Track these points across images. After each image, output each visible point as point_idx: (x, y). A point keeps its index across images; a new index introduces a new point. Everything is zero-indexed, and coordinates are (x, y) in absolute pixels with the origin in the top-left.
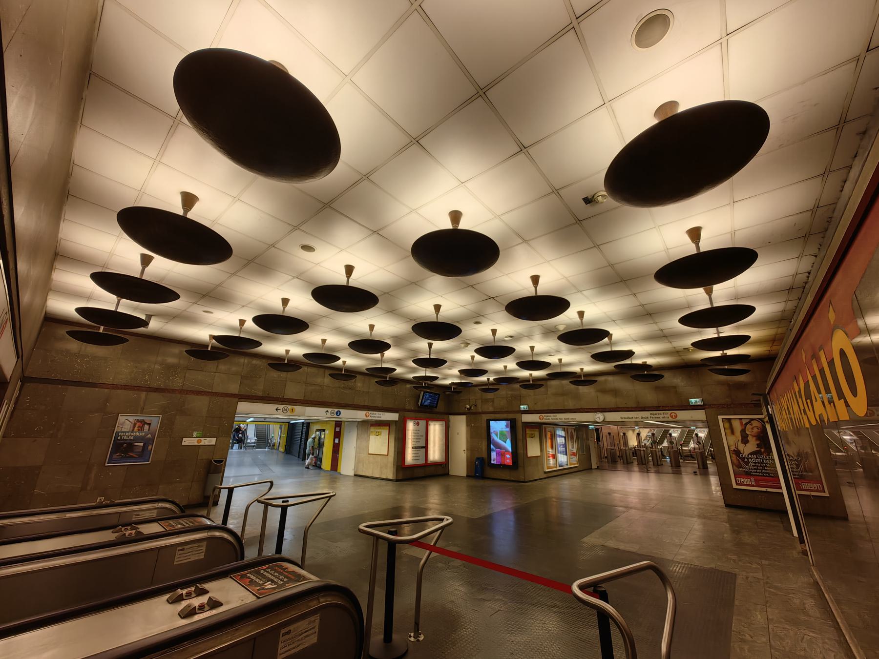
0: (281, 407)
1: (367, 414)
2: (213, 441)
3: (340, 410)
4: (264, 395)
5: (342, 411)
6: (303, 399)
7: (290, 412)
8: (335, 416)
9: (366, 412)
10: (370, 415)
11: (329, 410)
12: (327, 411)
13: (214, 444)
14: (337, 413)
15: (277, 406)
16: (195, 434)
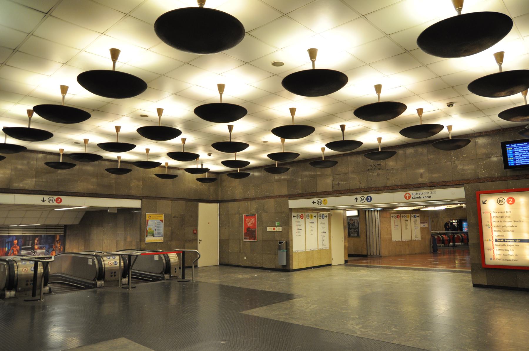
0: (316, 200)
1: (407, 195)
2: (279, 229)
3: (372, 195)
5: (372, 196)
6: (331, 190)
7: (324, 204)
8: (366, 202)
9: (405, 193)
10: (412, 196)
11: (359, 197)
12: (356, 198)
13: (281, 231)
14: (367, 199)
15: (312, 200)
16: (277, 224)
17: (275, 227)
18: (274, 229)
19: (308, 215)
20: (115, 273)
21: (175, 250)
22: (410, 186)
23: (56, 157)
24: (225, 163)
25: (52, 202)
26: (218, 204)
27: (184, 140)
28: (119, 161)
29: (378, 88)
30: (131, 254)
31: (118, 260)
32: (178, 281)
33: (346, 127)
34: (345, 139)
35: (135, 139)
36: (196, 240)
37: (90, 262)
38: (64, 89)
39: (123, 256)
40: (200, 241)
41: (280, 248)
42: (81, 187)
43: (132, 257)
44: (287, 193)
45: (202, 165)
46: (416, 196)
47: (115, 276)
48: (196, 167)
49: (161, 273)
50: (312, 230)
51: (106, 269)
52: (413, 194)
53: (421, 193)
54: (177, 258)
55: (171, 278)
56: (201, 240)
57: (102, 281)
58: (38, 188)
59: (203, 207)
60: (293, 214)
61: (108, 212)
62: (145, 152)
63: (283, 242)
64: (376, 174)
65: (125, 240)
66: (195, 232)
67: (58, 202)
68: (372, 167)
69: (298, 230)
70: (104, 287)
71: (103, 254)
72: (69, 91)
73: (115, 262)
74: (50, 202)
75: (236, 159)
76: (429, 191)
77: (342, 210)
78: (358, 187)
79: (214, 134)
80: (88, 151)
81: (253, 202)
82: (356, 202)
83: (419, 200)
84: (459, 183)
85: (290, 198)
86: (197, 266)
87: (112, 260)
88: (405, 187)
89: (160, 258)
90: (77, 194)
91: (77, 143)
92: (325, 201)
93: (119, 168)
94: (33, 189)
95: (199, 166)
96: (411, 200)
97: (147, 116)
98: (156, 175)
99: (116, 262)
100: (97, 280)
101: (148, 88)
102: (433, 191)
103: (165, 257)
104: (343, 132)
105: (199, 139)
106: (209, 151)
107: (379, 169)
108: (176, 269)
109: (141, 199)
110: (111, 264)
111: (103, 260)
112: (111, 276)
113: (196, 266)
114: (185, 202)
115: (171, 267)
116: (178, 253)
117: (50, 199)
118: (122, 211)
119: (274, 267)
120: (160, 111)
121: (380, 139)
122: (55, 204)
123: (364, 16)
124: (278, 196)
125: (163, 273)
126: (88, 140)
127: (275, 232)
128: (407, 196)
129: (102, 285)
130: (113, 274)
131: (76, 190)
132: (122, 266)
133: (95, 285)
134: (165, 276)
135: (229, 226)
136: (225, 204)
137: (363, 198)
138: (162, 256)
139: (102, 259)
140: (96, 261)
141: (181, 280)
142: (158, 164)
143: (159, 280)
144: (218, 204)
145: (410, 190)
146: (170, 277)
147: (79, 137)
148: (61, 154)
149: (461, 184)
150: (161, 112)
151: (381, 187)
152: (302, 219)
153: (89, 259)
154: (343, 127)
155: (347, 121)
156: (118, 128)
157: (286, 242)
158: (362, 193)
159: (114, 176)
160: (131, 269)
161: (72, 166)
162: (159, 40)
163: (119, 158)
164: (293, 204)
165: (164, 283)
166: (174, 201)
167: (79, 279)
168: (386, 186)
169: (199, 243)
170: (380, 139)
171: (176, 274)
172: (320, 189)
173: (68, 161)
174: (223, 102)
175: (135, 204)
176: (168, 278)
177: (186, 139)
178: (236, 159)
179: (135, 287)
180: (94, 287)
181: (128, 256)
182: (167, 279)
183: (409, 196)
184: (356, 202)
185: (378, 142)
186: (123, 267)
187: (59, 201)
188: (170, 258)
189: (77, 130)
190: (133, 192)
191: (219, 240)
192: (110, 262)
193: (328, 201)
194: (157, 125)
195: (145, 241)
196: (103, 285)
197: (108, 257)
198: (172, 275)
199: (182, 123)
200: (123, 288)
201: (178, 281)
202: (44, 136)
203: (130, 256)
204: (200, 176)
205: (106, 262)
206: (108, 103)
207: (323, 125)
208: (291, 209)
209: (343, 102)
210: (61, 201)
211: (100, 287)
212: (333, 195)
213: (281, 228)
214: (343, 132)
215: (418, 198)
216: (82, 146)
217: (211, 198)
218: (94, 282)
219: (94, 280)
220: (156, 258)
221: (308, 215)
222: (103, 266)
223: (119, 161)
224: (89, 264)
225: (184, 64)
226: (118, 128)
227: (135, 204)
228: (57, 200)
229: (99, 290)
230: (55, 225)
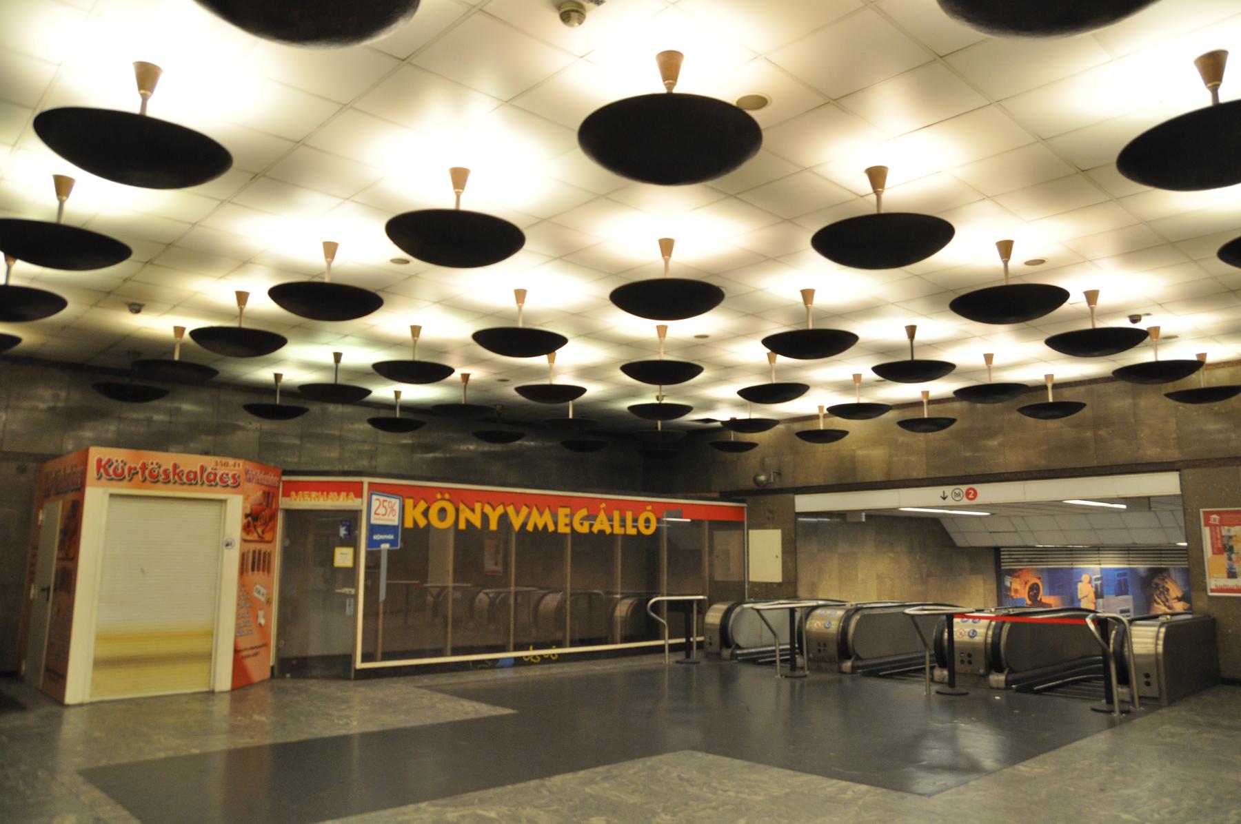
42: (1012, 460)
58: (933, 474)
67: (971, 496)
75: (1093, 324)
90: (1006, 475)
94: (925, 476)
117: (955, 493)
129: (943, 679)
178: (1093, 324)
187: (971, 495)
192: (961, 631)
195: (1205, 589)
202: (794, 390)
227: (1166, 484)
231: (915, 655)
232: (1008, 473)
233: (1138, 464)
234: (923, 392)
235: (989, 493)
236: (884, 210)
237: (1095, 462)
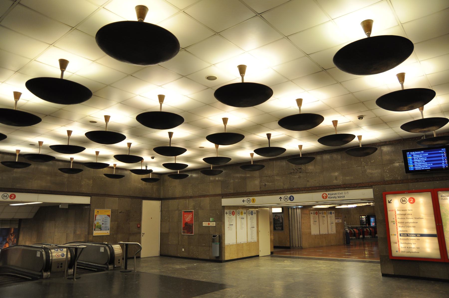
0: (245, 199)
1: (325, 195)
2: (213, 224)
3: (293, 195)
4: (234, 192)
5: (294, 195)
6: (259, 190)
8: (289, 201)
9: (323, 193)
10: (328, 196)
11: (282, 196)
12: (281, 198)
14: (290, 198)
15: (242, 199)
16: (211, 219)
17: (210, 223)
18: (209, 224)
19: (239, 212)
20: (62, 264)
21: (119, 243)
22: (327, 187)
23: (13, 157)
24: (166, 165)
25: (6, 198)
26: (161, 201)
27: (129, 144)
28: (72, 162)
29: (299, 102)
30: (77, 247)
31: (65, 252)
32: (121, 272)
33: (272, 136)
34: (271, 146)
35: (86, 142)
36: (140, 233)
37: (38, 255)
38: (17, 95)
39: (70, 248)
40: (143, 234)
41: (213, 241)
42: (35, 184)
43: (78, 249)
44: (220, 193)
45: (146, 167)
46: (332, 196)
47: (61, 267)
48: (141, 169)
49: (106, 264)
50: (242, 225)
51: (53, 261)
52: (330, 194)
53: (336, 193)
54: (120, 250)
55: (115, 269)
56: (144, 234)
57: (49, 272)
59: (146, 204)
60: (226, 211)
61: (60, 207)
62: (95, 154)
63: (217, 236)
64: (298, 176)
65: (75, 233)
66: (139, 226)
67: (12, 198)
68: (294, 171)
69: (230, 225)
70: (50, 278)
71: (52, 246)
72: (22, 97)
73: (62, 254)
74: (4, 198)
75: (175, 162)
76: (343, 192)
77: (268, 207)
78: (282, 188)
79: (157, 140)
80: (42, 152)
81: (191, 200)
82: (281, 201)
83: (334, 199)
84: (368, 185)
85: (223, 197)
86: (140, 257)
87: (60, 252)
88: (322, 188)
89: (105, 249)
91: (32, 145)
92: (253, 200)
93: (71, 168)
95: (144, 168)
96: (328, 199)
97: (96, 122)
98: (105, 175)
99: (63, 254)
100: (43, 272)
101: (93, 96)
102: (346, 191)
103: (110, 249)
104: (269, 140)
105: (143, 143)
106: (152, 155)
107: (300, 172)
108: (119, 260)
109: (91, 196)
110: (58, 256)
111: (51, 251)
112: (58, 267)
113: (139, 257)
114: (130, 199)
115: (115, 258)
116: (122, 245)
118: (72, 206)
119: (208, 258)
120: (107, 118)
121: (301, 147)
122: (9, 200)
123: (287, 37)
124: (213, 195)
125: (108, 264)
126: (42, 142)
127: (210, 226)
128: (324, 196)
129: (48, 276)
130: (60, 266)
131: (29, 187)
132: (69, 258)
133: (41, 276)
134: (109, 266)
135: (169, 221)
136: (166, 202)
137: (286, 197)
138: (107, 248)
139: (50, 251)
140: (44, 253)
141: (124, 270)
142: (107, 165)
143: (103, 271)
144: (161, 201)
145: (327, 190)
146: (114, 267)
147: (35, 139)
148: (18, 154)
149: (369, 185)
150: (108, 119)
151: (302, 188)
152: (233, 215)
153: (38, 252)
154: (269, 136)
155: (272, 130)
156: (69, 132)
157: (219, 236)
158: (285, 193)
159: (66, 175)
160: (77, 260)
161: (26, 165)
162: (103, 53)
163: (71, 158)
164: (226, 202)
165: (108, 273)
166: (120, 198)
167: (26, 271)
168: (307, 187)
169: (142, 236)
170: (301, 147)
171: (119, 265)
172: (249, 189)
173: (24, 160)
174: (163, 110)
175: (86, 200)
176: (112, 268)
177: (131, 143)
179: (80, 278)
180: (40, 278)
181: (74, 249)
182: (111, 270)
183: (326, 196)
184: (281, 201)
185: (300, 149)
186: (70, 259)
188: (115, 250)
189: (33, 133)
190: (83, 190)
191: (160, 233)
192: (57, 254)
193: (256, 200)
194: (104, 130)
195: (92, 234)
196: (49, 276)
197: (56, 250)
198: (115, 266)
199: (127, 129)
200: (68, 278)
201: (121, 272)
203: (76, 249)
204: (144, 176)
205: (54, 254)
206: (60, 109)
207: (252, 134)
208: (224, 207)
209: (269, 113)
210: (15, 197)
211: (47, 278)
212: (261, 194)
213: (215, 223)
214: (269, 140)
215: (334, 197)
216: (37, 147)
217: (154, 196)
218: (40, 274)
219: (41, 271)
220: (102, 250)
221: (239, 212)
222: (51, 258)
223: (72, 162)
224: (37, 256)
225: (128, 75)
226: (69, 132)
227: (86, 200)
228: (11, 197)
229: (44, 281)
230: (10, 219)
231: (92, 264)
232: (32, 190)
233: (79, 193)
234: (114, 164)
235: (20, 196)
236: (163, 110)
237: (66, 190)
